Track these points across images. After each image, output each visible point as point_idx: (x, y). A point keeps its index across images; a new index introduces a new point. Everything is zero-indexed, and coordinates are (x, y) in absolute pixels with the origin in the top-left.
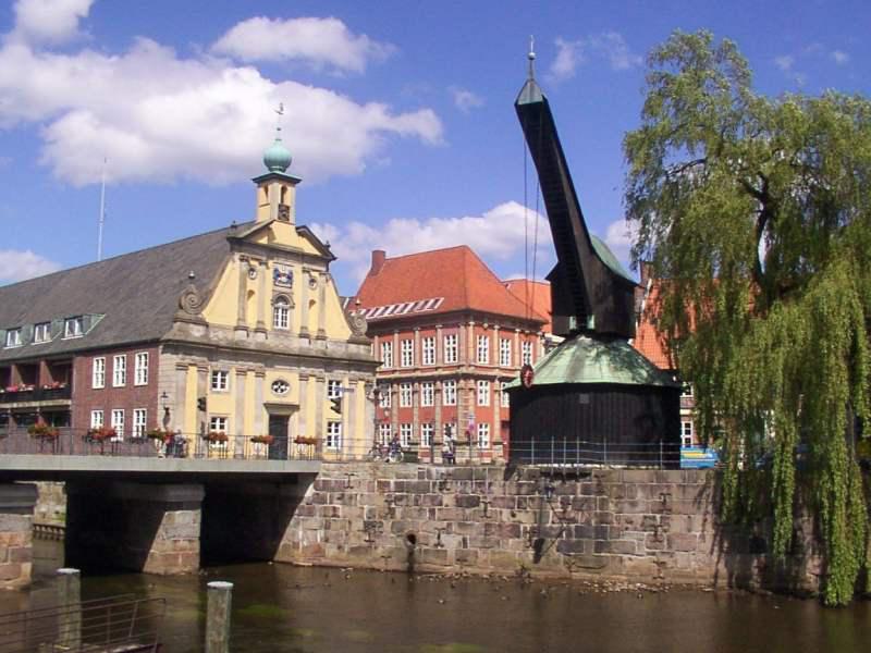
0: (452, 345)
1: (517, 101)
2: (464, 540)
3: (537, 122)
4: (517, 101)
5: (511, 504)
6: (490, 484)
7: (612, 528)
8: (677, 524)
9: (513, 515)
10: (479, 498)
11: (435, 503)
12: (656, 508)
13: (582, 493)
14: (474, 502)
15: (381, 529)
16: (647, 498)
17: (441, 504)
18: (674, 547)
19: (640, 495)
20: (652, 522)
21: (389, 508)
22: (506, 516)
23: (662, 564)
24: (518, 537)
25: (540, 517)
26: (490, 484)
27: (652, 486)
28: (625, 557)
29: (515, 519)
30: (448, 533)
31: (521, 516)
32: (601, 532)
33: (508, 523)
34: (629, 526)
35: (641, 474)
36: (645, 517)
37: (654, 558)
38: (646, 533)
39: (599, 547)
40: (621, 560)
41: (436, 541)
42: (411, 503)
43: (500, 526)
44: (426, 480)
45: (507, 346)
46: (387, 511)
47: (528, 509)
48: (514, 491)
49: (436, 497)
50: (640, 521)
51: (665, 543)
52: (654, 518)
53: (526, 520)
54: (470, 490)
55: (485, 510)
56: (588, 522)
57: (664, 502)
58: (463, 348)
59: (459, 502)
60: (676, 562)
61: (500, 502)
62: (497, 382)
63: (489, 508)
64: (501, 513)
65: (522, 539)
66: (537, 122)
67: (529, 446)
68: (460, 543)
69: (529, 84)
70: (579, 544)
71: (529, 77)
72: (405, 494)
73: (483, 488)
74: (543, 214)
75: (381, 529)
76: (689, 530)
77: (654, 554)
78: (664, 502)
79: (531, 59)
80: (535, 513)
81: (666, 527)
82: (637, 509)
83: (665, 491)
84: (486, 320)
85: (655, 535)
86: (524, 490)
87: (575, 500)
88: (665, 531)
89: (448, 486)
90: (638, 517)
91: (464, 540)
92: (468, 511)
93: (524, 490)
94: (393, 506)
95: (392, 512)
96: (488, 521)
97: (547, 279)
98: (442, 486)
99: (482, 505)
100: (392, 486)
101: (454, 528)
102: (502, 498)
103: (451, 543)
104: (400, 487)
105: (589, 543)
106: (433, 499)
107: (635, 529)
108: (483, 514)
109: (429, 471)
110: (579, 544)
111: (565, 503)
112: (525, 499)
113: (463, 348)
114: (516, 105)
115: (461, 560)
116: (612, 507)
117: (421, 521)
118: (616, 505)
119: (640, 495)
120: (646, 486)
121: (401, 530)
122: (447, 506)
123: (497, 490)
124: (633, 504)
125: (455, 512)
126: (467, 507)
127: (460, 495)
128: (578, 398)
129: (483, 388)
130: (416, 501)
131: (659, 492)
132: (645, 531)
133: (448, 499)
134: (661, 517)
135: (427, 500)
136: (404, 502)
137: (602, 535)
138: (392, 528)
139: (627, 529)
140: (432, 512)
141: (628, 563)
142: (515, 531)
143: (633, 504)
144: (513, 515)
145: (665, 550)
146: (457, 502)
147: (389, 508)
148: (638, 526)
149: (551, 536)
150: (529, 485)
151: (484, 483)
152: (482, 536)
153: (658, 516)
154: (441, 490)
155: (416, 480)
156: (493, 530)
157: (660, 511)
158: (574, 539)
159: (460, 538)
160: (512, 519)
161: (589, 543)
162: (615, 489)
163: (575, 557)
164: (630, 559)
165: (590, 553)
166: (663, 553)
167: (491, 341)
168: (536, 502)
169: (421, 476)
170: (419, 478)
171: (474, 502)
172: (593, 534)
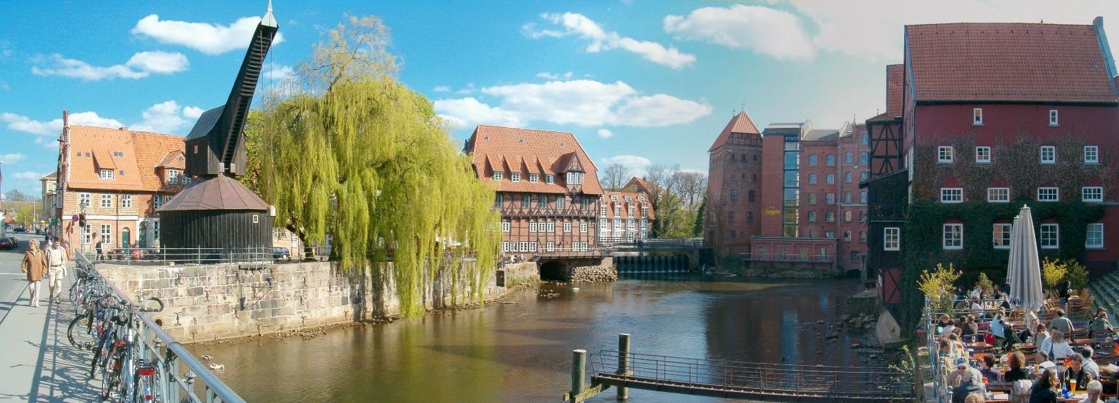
8: (310, 295)
14: (199, 291)
31: (229, 299)
32: (274, 303)
39: (274, 313)
48: (224, 281)
53: (233, 301)
59: (189, 293)
86: (231, 280)
90: (292, 293)
92: (196, 298)
93: (231, 280)
98: (178, 281)
100: (140, 285)
101: (188, 311)
103: (186, 322)
104: (146, 284)
105: (269, 310)
106: (171, 292)
111: (254, 288)
123: (214, 283)
125: (188, 301)
133: (182, 290)
137: (274, 305)
140: (171, 301)
142: (226, 308)
143: (290, 285)
159: (191, 318)
161: (269, 310)
165: (269, 317)
169: (161, 275)
171: (199, 291)
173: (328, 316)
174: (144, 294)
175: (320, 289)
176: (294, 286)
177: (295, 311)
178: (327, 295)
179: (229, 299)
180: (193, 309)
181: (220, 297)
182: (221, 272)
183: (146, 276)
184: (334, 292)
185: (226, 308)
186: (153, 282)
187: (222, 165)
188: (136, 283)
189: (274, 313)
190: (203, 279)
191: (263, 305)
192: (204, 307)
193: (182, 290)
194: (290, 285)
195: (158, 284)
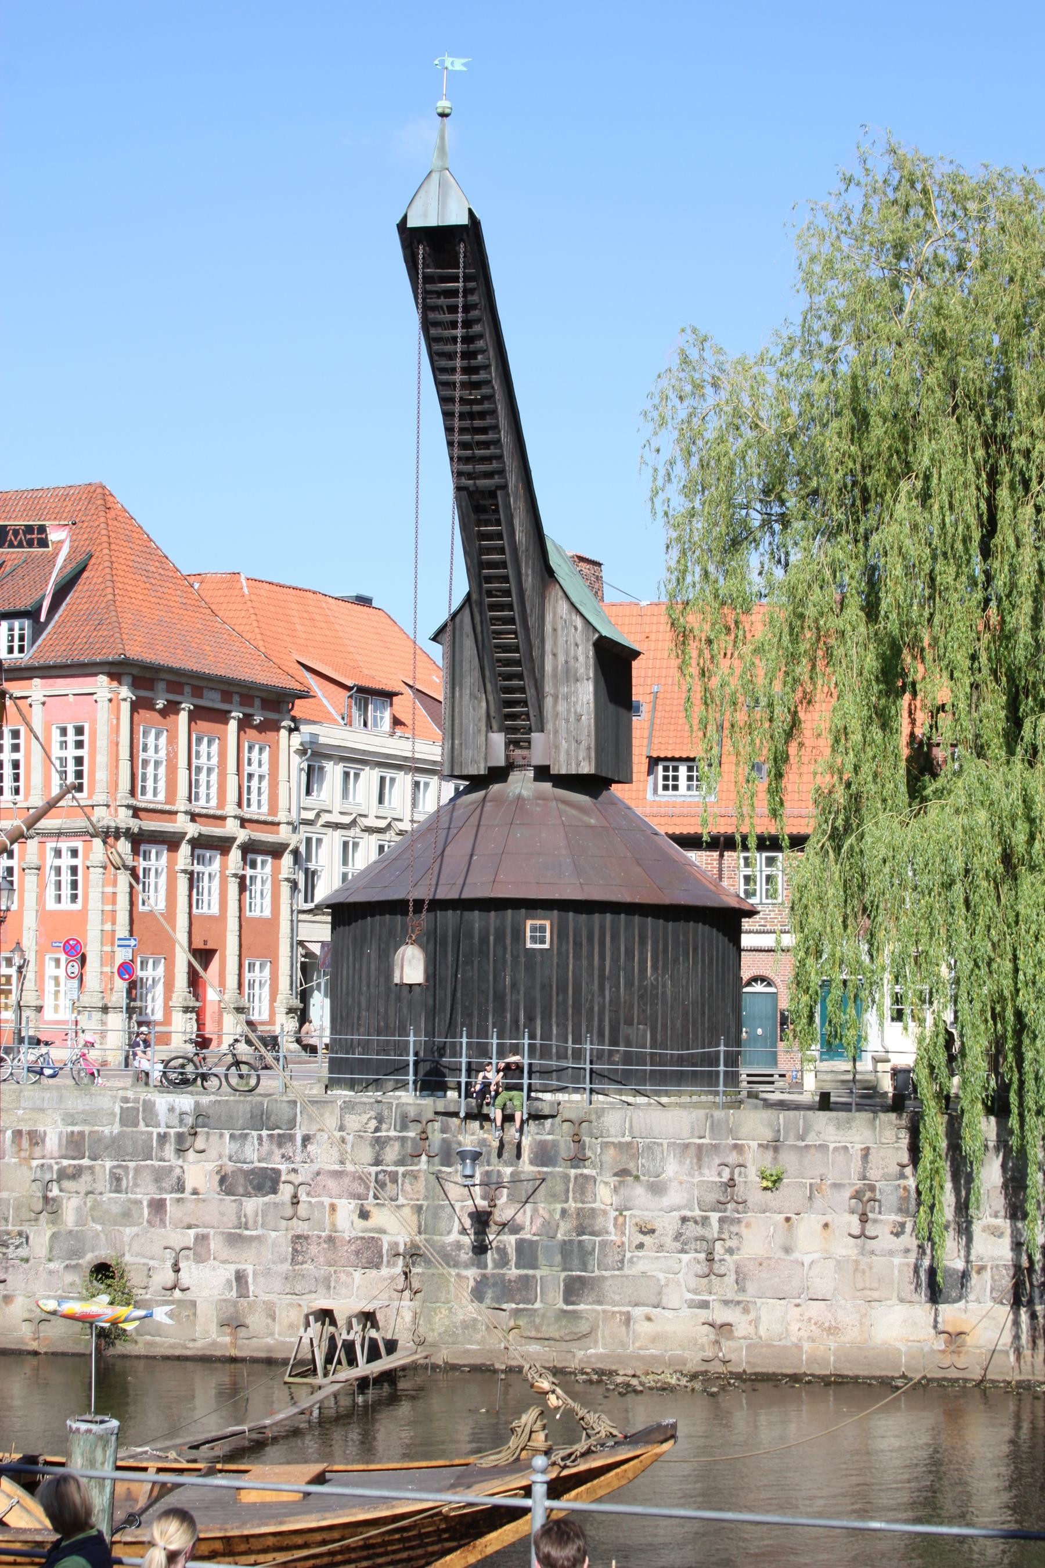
0: (72, 752)
1: (405, 219)
2: (240, 1277)
3: (447, 264)
4: (405, 219)
5: (361, 1190)
6: (306, 1139)
7: (604, 1244)
9: (364, 1215)
10: (278, 1172)
11: (166, 1185)
12: (712, 1197)
13: (531, 1163)
14: (265, 1182)
15: (23, 1252)
16: (690, 1174)
17: (180, 1187)
18: (751, 1287)
19: (672, 1168)
20: (699, 1231)
21: (46, 1198)
22: (346, 1218)
23: (724, 1329)
24: (378, 1267)
25: (428, 1217)
26: (306, 1139)
27: (700, 1147)
28: (638, 1312)
29: (370, 1223)
30: (199, 1259)
31: (380, 1217)
32: (574, 1253)
33: (346, 1236)
34: (647, 1240)
35: (665, 1119)
36: (684, 1220)
37: (704, 1315)
38: (683, 1256)
39: (574, 1290)
40: (628, 1319)
41: (167, 1276)
42: (103, 1183)
43: (331, 1240)
44: (142, 1127)
45: (207, 754)
46: (39, 1205)
47: (401, 1200)
48: (367, 1154)
49: (171, 1169)
50: (671, 1231)
51: (731, 1279)
52: (706, 1219)
53: (395, 1226)
54: (255, 1152)
55: (295, 1201)
56: (549, 1229)
57: (731, 1184)
58: (102, 759)
59: (226, 1183)
60: (756, 1323)
61: (332, 1184)
62: (185, 849)
63: (303, 1197)
64: (333, 1208)
65: (385, 1271)
66: (447, 264)
67: (403, 1048)
68: (229, 1281)
69: (435, 177)
70: (526, 1282)
71: (435, 162)
72: (86, 1162)
73: (288, 1150)
74: (558, 548)
75: (23, 1252)
76: (787, 1250)
77: (705, 1305)
78: (731, 1184)
79: (443, 115)
80: (419, 1208)
81: (729, 1243)
82: (667, 1201)
83: (732, 1158)
84: (161, 686)
85: (710, 1260)
86: (391, 1153)
87: (516, 1179)
88: (730, 1251)
89: (200, 1143)
90: (667, 1224)
91: (240, 1277)
92: (252, 1205)
93: (391, 1153)
94: (55, 1192)
95: (50, 1206)
96: (301, 1227)
97: (435, 639)
99: (285, 1192)
100: (52, 1143)
101: (215, 1244)
102: (338, 1174)
103: (208, 1282)
104: (75, 1144)
105: (550, 1275)
106: (159, 1176)
107: (661, 1248)
108: (289, 1212)
109: (149, 1107)
110: (526, 1282)
112: (394, 1178)
113: (102, 759)
114: (402, 226)
115: (233, 1323)
116: (604, 1195)
117: (129, 1231)
118: (616, 1190)
119: (672, 1168)
120: (687, 1146)
121: (76, 1253)
122: (195, 1192)
123: (323, 1155)
124: (657, 1189)
125: (220, 1211)
126: (248, 1195)
127: (230, 1167)
128: (518, 935)
129: (153, 863)
130: (116, 1180)
131: (717, 1161)
132: (683, 1251)
133: (198, 1172)
134: (721, 1220)
135: (147, 1177)
136: (83, 1183)
138: (51, 1250)
139: (641, 1246)
140: (158, 1206)
141: (643, 1328)
142: (369, 1253)
144: (364, 1215)
145: (730, 1296)
146: (222, 1180)
147: (46, 1198)
148: (668, 1241)
149: (456, 1265)
150: (403, 1140)
151: (291, 1138)
152: (286, 1267)
153: (714, 1217)
154: (180, 1151)
155: (116, 1129)
156: (314, 1249)
157: (720, 1205)
158: (513, 1272)
159: (228, 1272)
160: (361, 1223)
162: (612, 1151)
163: (517, 1312)
164: (649, 1319)
166: (726, 1303)
167: (172, 741)
168: (421, 1185)
169: (128, 1118)
170: (123, 1122)
171: (265, 1182)
172: (558, 1259)
173: (851, 1335)
174: (63, 1175)
175: (808, 1225)
176: (675, 1196)
177: (675, 1297)
178: (847, 1248)
179: (380, 1217)
180: (234, 1240)
181: (347, 1208)
182: (353, 1122)
183: (70, 1119)
184: (886, 1241)
185: (369, 1253)
186: (97, 1139)
187: (498, 739)
188: (36, 1139)
189: (574, 1290)
190: (281, 1141)
191: (527, 1254)
192: (279, 1238)
193: (198, 1172)
194: (657, 1189)
195: (116, 1147)
